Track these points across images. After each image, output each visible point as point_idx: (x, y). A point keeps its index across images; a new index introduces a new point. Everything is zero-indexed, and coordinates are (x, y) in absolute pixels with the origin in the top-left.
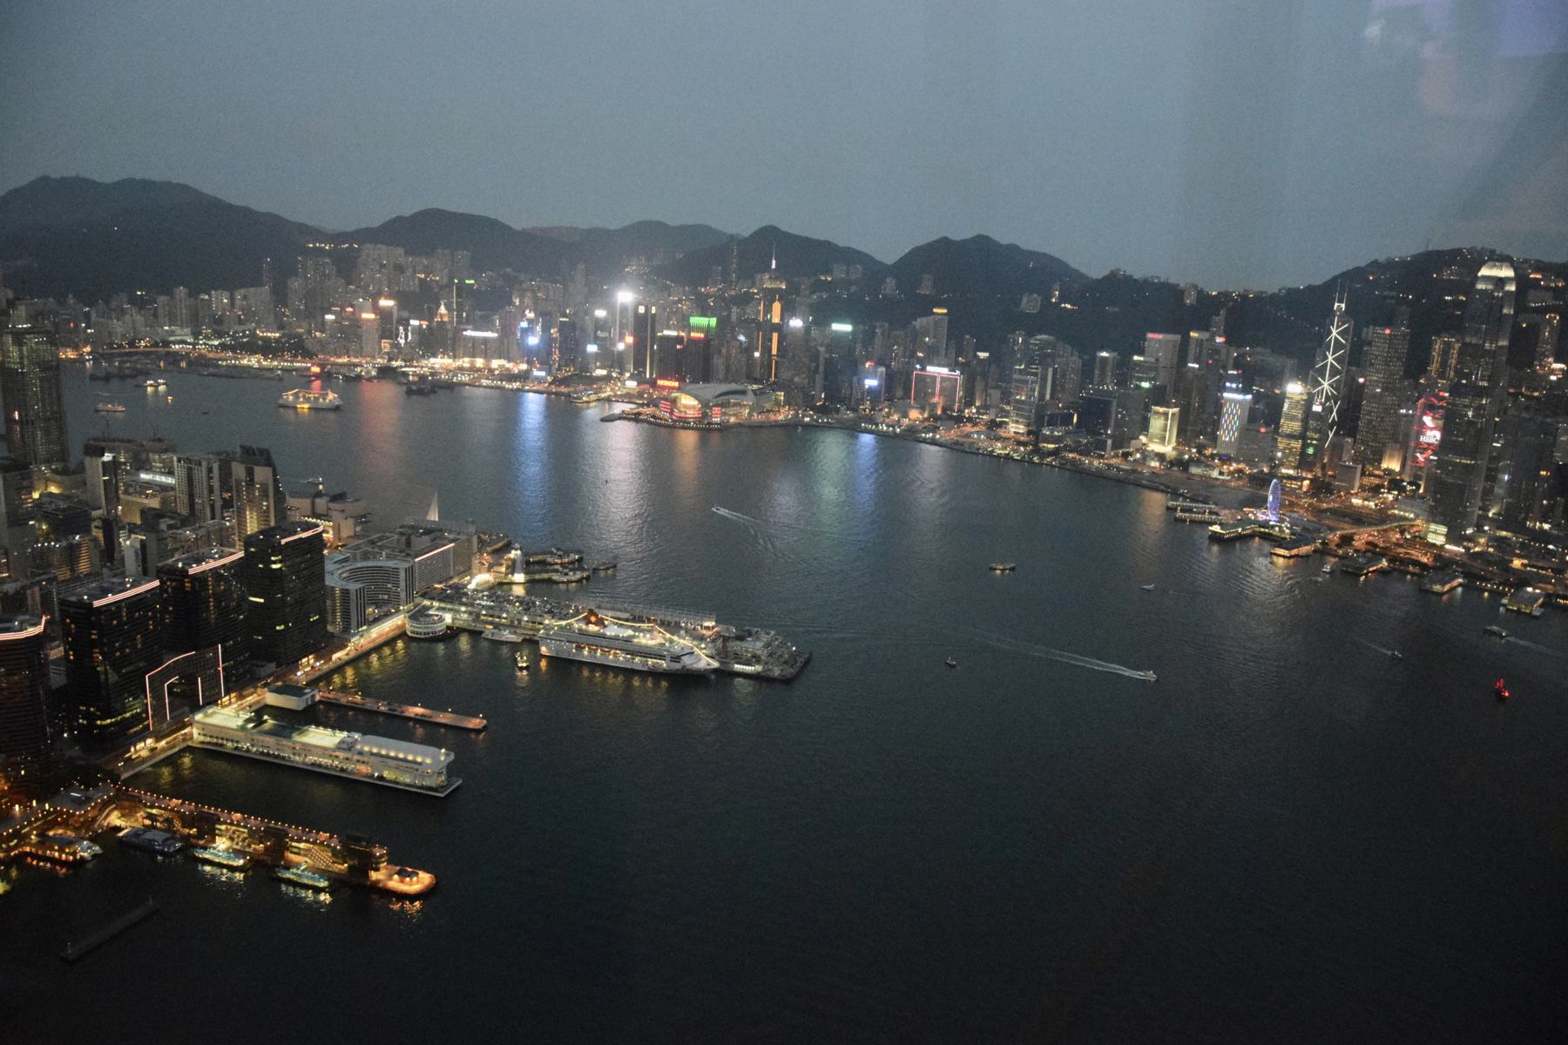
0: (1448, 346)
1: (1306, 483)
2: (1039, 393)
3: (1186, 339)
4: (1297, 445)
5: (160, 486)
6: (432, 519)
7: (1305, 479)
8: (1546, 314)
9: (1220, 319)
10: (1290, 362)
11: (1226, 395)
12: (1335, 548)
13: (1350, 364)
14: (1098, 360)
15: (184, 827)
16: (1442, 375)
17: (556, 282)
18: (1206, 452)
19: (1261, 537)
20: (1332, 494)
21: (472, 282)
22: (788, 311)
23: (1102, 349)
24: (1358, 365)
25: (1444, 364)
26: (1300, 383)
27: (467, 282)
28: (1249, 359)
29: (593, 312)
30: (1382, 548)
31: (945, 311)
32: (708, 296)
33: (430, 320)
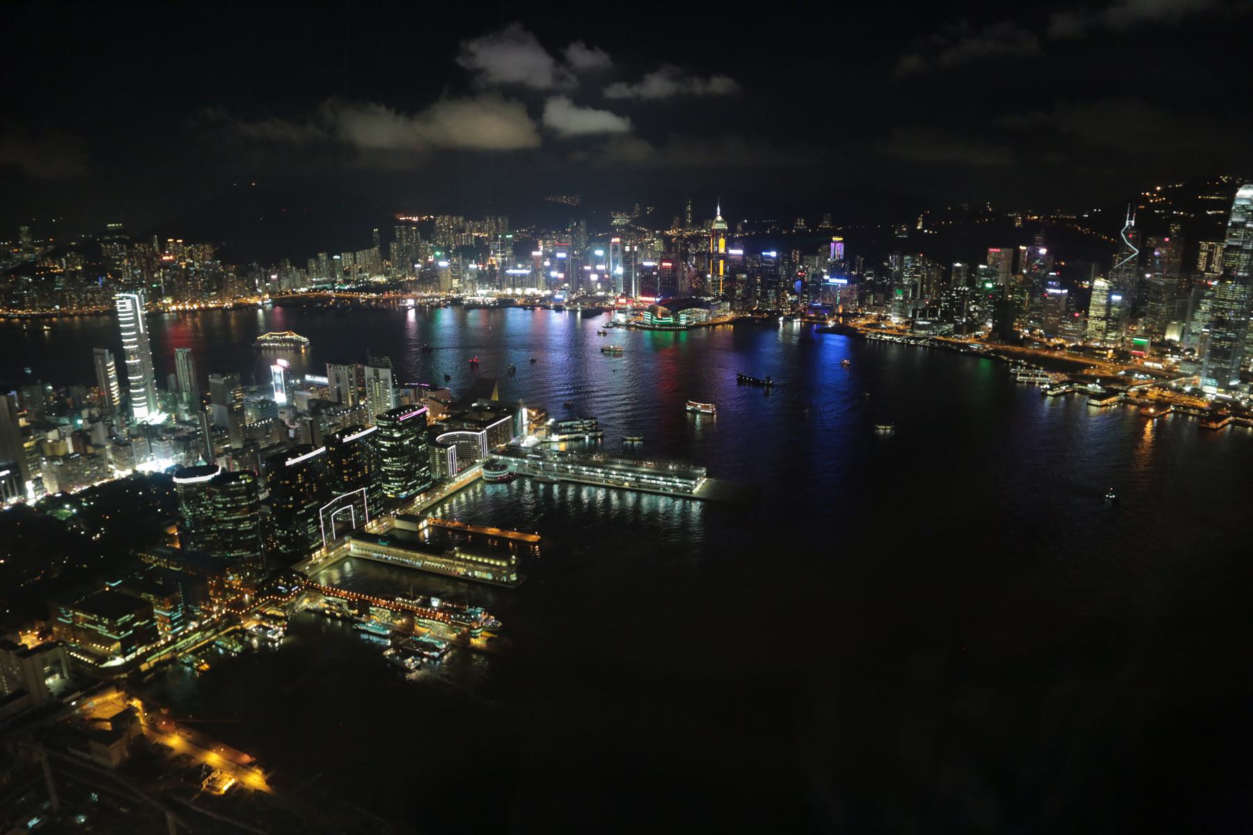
0: (1211, 247)
1: (1111, 351)
2: (912, 295)
4: (1103, 324)
5: (319, 384)
6: (494, 399)
7: (1110, 349)
12: (1135, 399)
13: (1139, 265)
14: (954, 271)
15: (349, 609)
16: (1208, 270)
17: (567, 233)
19: (1079, 392)
20: (1129, 359)
21: (511, 236)
22: (729, 244)
23: (956, 263)
26: (1103, 279)
27: (507, 236)
29: (593, 252)
31: (841, 239)
32: (672, 237)
33: (484, 264)
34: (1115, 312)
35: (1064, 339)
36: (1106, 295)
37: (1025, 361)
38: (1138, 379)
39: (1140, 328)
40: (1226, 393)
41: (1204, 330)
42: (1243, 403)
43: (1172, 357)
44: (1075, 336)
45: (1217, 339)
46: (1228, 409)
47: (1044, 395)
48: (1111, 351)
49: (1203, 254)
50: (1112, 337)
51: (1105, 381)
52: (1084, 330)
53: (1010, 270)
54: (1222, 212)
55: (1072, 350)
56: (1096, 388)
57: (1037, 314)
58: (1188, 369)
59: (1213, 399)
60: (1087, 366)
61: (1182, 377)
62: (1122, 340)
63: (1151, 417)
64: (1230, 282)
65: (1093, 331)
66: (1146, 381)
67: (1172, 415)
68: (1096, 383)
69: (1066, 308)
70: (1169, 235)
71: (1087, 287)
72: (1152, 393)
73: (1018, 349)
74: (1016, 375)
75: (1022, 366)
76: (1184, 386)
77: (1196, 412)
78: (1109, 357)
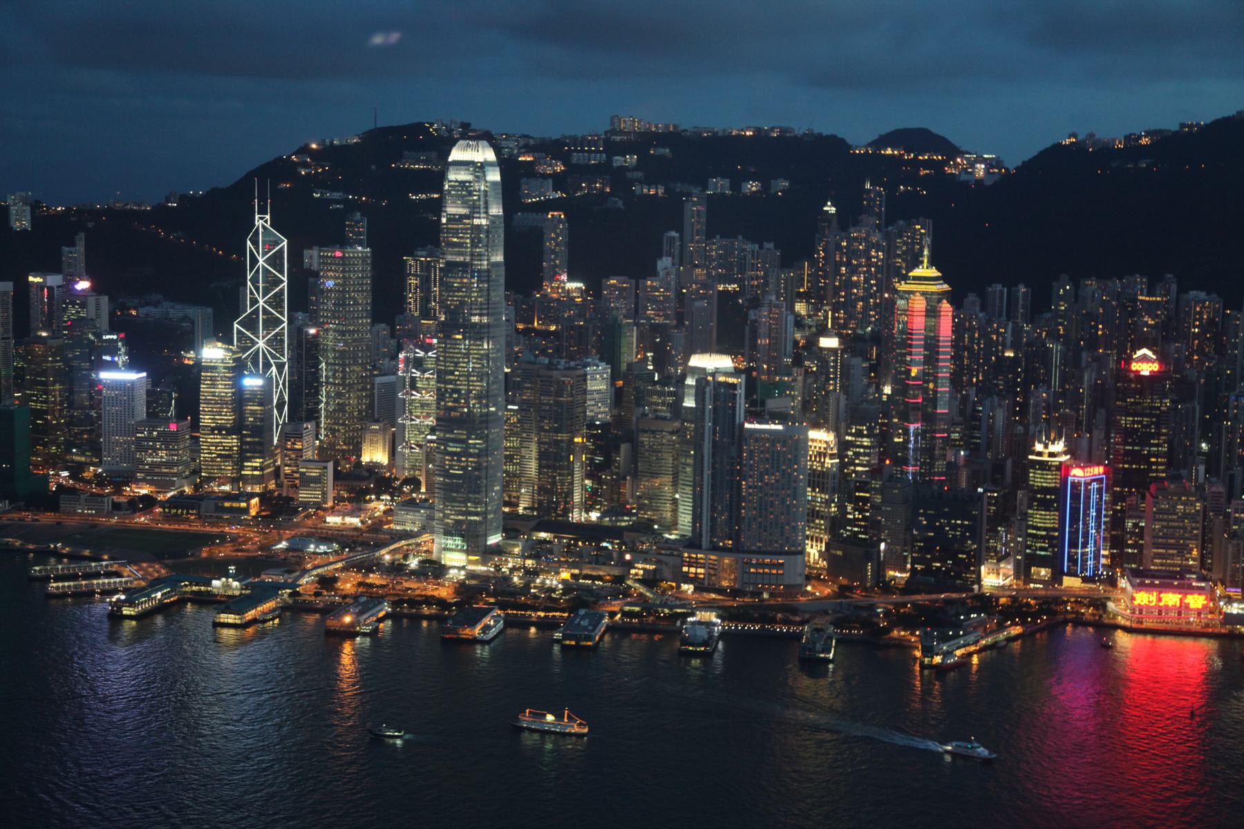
0: (427, 267)
1: (255, 501)
3: (23, 289)
4: (233, 441)
7: (252, 495)
8: (548, 214)
9: (76, 253)
10: (200, 314)
11: (105, 375)
12: (313, 598)
16: (426, 313)
18: (85, 475)
19: (194, 602)
20: (295, 512)
24: (305, 310)
25: (426, 300)
26: (220, 344)
28: (134, 313)
30: (377, 587)
34: (253, 413)
35: (151, 483)
36: (230, 379)
37: (65, 545)
38: (314, 553)
39: (309, 446)
40: (484, 563)
41: (429, 437)
42: (516, 579)
43: (378, 499)
44: (174, 475)
45: (452, 454)
46: (489, 595)
47: (116, 617)
48: (255, 501)
49: (413, 281)
50: (255, 469)
51: (248, 567)
52: (194, 460)
53: (11, 335)
54: (436, 196)
55: (170, 508)
56: (227, 586)
57: (82, 432)
58: (409, 521)
59: (462, 577)
60: (208, 539)
61: (400, 539)
62: (277, 473)
63: (350, 634)
64: (460, 337)
65: (213, 460)
66: (331, 559)
67: (389, 623)
68: (227, 576)
69: (148, 414)
70: (343, 242)
71: (191, 363)
72: (346, 582)
73: (47, 518)
74: (47, 579)
75: (59, 556)
76: (406, 557)
77: (434, 610)
78: (253, 512)
